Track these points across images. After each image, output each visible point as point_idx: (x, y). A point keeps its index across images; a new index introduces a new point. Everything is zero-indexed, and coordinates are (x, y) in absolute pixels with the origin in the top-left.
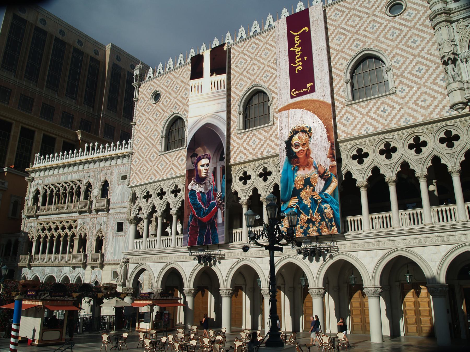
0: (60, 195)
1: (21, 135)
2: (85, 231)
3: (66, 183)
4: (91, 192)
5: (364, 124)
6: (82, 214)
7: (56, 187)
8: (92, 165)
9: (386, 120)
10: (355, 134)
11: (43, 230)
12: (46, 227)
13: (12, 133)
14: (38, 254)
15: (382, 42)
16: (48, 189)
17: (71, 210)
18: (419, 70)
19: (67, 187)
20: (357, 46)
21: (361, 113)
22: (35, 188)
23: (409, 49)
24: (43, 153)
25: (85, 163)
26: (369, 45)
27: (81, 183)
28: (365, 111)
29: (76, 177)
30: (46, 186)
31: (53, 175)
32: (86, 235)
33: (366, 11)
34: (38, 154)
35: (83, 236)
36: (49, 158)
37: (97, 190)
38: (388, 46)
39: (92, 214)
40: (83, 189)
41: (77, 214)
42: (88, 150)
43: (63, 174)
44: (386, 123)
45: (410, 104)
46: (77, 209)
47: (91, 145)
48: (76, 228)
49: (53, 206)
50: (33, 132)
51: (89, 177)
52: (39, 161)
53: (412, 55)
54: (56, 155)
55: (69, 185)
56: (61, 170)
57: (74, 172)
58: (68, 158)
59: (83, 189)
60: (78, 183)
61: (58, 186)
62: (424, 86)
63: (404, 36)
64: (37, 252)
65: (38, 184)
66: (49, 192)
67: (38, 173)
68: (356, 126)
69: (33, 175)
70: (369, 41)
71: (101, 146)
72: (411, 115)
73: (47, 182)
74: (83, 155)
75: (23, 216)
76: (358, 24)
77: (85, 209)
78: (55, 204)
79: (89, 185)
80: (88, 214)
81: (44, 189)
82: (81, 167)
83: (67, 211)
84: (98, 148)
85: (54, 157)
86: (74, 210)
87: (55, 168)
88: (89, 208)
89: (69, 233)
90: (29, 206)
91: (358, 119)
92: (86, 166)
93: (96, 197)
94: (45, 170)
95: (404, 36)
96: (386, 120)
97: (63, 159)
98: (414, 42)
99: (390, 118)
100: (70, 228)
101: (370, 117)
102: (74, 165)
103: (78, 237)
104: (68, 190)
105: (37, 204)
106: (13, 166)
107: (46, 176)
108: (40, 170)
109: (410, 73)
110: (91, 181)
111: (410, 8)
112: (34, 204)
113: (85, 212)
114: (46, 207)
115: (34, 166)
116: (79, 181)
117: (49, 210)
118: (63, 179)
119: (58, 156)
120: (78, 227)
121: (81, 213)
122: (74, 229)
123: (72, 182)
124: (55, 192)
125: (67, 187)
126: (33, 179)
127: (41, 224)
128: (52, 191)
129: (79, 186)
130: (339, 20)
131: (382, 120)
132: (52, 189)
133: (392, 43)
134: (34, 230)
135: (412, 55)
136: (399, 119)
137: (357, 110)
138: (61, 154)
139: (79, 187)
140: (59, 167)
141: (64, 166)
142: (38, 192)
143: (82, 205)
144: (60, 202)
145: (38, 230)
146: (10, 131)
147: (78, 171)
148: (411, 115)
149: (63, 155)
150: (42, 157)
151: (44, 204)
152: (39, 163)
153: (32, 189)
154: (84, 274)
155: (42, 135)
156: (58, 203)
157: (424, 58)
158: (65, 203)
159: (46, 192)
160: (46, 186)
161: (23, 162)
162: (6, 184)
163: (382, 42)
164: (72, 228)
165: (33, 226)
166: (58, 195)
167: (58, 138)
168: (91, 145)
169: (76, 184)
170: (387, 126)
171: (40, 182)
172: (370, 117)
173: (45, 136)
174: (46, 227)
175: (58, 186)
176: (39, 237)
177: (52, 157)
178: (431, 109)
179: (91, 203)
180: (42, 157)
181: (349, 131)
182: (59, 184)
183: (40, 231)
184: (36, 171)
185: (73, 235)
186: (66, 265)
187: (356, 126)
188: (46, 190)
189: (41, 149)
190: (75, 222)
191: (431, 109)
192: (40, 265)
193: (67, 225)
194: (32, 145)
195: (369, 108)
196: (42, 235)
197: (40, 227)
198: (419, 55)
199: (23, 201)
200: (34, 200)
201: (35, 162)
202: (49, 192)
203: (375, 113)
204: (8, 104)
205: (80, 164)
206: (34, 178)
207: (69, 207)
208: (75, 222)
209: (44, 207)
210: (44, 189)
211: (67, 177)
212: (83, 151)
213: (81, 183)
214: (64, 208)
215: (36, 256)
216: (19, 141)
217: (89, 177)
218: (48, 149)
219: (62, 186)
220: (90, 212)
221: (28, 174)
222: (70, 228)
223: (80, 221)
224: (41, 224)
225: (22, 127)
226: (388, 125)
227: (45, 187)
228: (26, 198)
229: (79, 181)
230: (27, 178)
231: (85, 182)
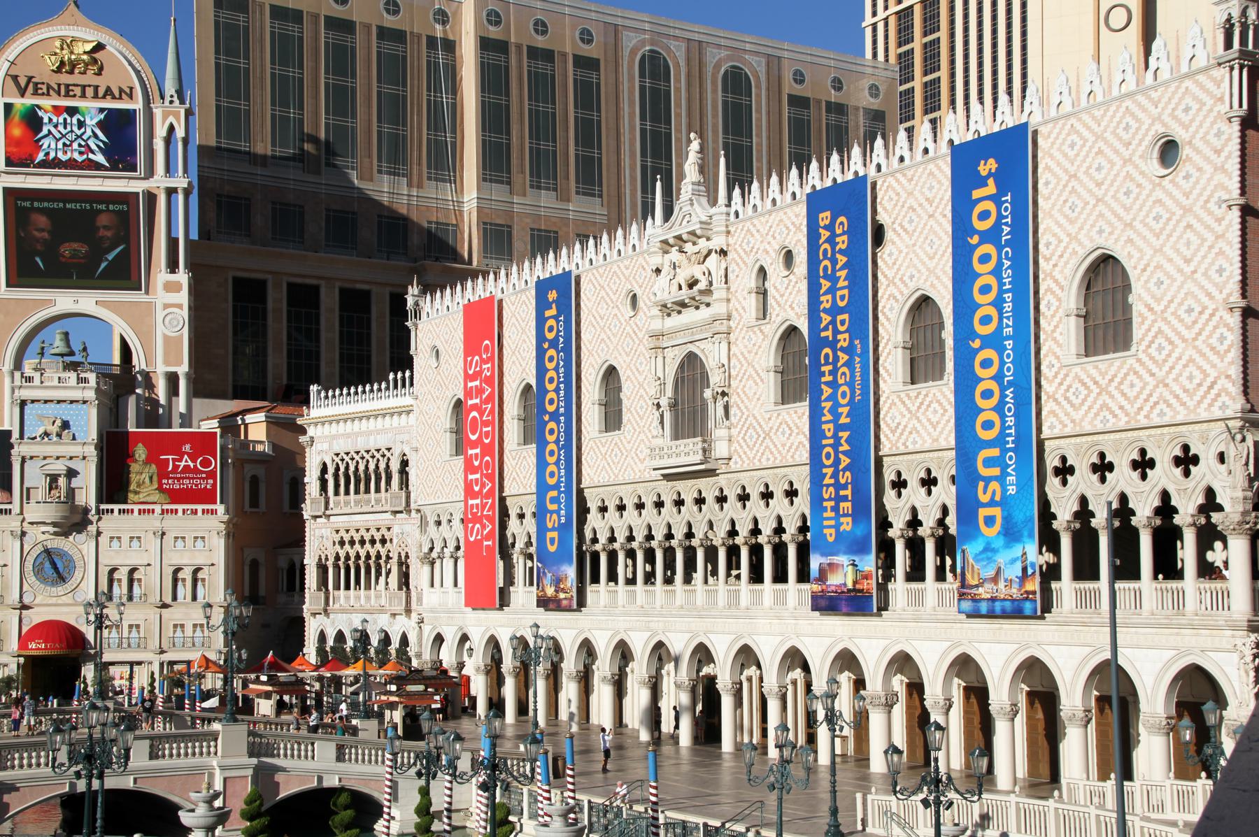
1: (289, 304)
11: (342, 543)
12: (347, 538)
13: (270, 305)
14: (339, 589)
30: (337, 455)
32: (407, 557)
40: (395, 466)
50: (316, 289)
64: (337, 587)
100: (383, 541)
103: (395, 559)
120: (395, 541)
127: (337, 531)
142: (324, 469)
146: (263, 300)
155: (337, 291)
167: (374, 289)
171: (325, 446)
173: (343, 292)
174: (347, 538)
176: (337, 558)
180: (323, 394)
183: (338, 547)
186: (382, 610)
192: (343, 611)
193: (378, 537)
194: (318, 323)
197: (337, 539)
208: (389, 529)
215: (336, 593)
216: (289, 321)
220: (409, 512)
222: (383, 541)
223: (396, 530)
224: (337, 531)
225: (290, 285)
229: (389, 449)
231: (397, 452)
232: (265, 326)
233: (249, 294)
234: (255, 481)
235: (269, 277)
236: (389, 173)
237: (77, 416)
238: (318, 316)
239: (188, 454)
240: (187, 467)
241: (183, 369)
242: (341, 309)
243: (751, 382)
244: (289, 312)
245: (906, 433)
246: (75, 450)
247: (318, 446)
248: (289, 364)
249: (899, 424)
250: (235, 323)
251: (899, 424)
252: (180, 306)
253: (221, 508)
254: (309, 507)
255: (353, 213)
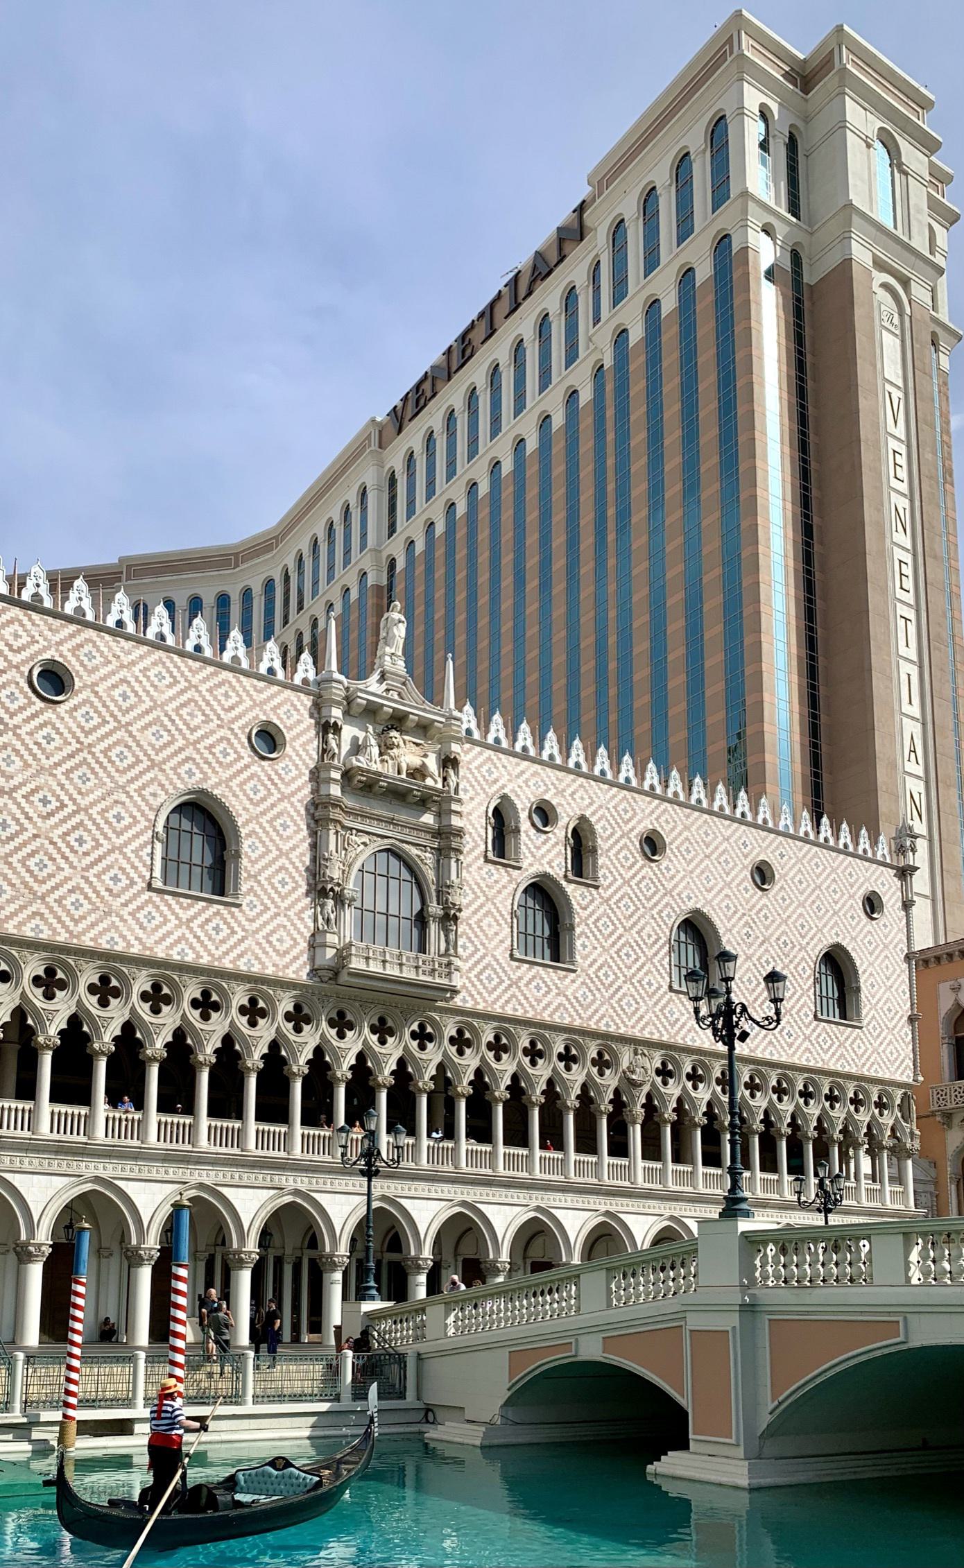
5: (178, 941)
9: (217, 948)
10: (160, 953)
15: (235, 795)
18: (283, 883)
20: (190, 773)
21: (177, 918)
23: (273, 834)
26: (213, 787)
28: (184, 915)
33: (220, 711)
38: (244, 809)
44: (218, 953)
45: (259, 936)
53: (278, 849)
62: (285, 915)
63: (273, 806)
68: (163, 939)
70: (214, 780)
72: (257, 958)
76: (199, 728)
91: (169, 926)
95: (273, 806)
96: (217, 948)
98: (285, 827)
99: (224, 948)
101: (191, 930)
109: (268, 879)
111: (290, 757)
130: (163, 692)
131: (211, 947)
133: (251, 807)
135: (278, 849)
136: (240, 956)
137: (169, 906)
148: (257, 958)
157: (293, 863)
163: (235, 795)
170: (217, 959)
172: (191, 930)
178: (288, 959)
181: (150, 942)
187: (163, 939)
191: (288, 959)
195: (192, 912)
198: (287, 855)
203: (201, 926)
226: (220, 959)
243: (489, 919)
245: (685, 1030)
249: (678, 1020)
251: (678, 1020)
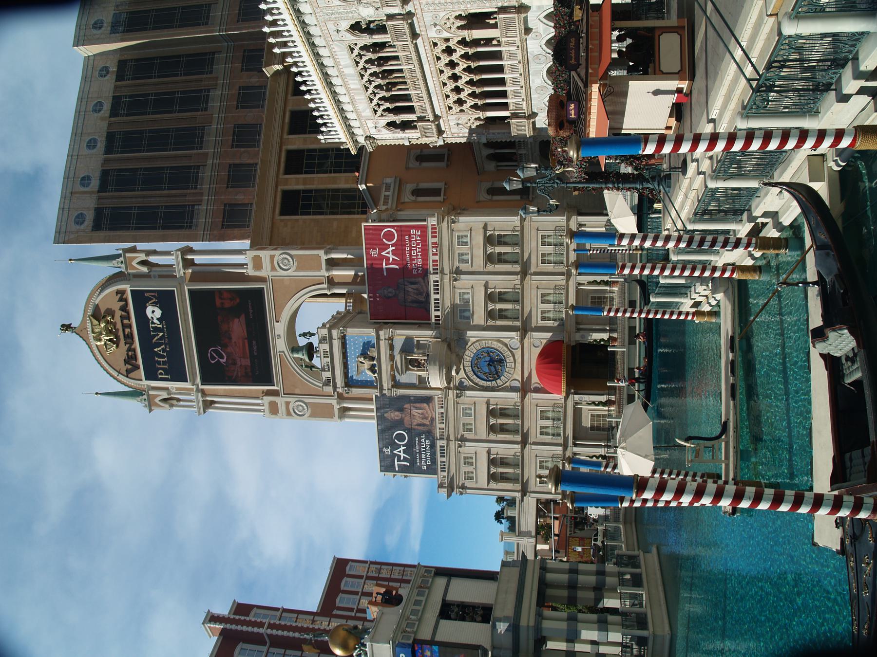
0: (388, 84)
2: (452, 20)
3: (362, 76)
4: (371, 22)
6: (418, 32)
7: (374, 94)
8: (312, 30)
11: (460, 102)
12: (454, 97)
13: (300, 187)
14: (506, 104)
16: (382, 108)
17: (414, 56)
19: (369, 71)
22: (385, 131)
24: (316, 129)
25: (313, 45)
27: (356, 44)
29: (345, 59)
31: (352, 102)
32: (459, 17)
34: (320, 137)
35: (462, 23)
36: (321, 117)
37: (361, 8)
39: (413, 11)
40: (367, 40)
41: (419, 41)
42: (285, 44)
43: (345, 85)
46: (409, 43)
47: (272, 40)
48: (447, 40)
49: (411, 92)
50: (289, 152)
51: (338, 31)
52: (333, 133)
54: (312, 105)
55: (365, 69)
56: (338, 90)
57: (337, 65)
58: (312, 81)
59: (367, 40)
60: (356, 52)
61: (370, 90)
65: (376, 127)
66: (387, 105)
67: (356, 131)
69: (361, 140)
71: (269, 18)
73: (368, 113)
74: (298, 52)
75: (441, 143)
77: (406, 26)
78: (407, 89)
79: (356, 27)
80: (415, 19)
81: (382, 115)
82: (322, 52)
83: (416, 63)
84: (274, 23)
85: (317, 109)
86: (412, 49)
87: (338, 102)
88: (403, 19)
89: (460, 51)
90: (419, 135)
92: (317, 41)
93: (377, 9)
94: (345, 119)
97: (316, 90)
100: (449, 51)
102: (322, 66)
103: (465, 34)
104: (374, 69)
105: (413, 121)
106: (357, 174)
107: (358, 115)
108: (349, 127)
110: (345, 25)
112: (415, 127)
113: (412, 26)
114: (415, 104)
115: (343, 140)
116: (352, 50)
117: (420, 99)
118: (356, 84)
119: (313, 100)
120: (446, 35)
121: (415, 35)
122: (450, 44)
123: (357, 63)
124: (383, 94)
125: (369, 71)
126: (368, 138)
127: (450, 108)
128: (383, 99)
129: (361, 48)
132: (380, 99)
134: (464, 118)
138: (307, 97)
139: (365, 48)
140: (334, 94)
141: (330, 85)
142: (391, 125)
143: (398, 35)
144: (401, 80)
145: (462, 111)
146: (297, 192)
147: (332, 56)
149: (309, 91)
150: (323, 129)
151: (411, 110)
152: (336, 133)
153: (388, 136)
154: (539, 7)
156: (405, 83)
158: (401, 71)
159: (387, 110)
160: (376, 111)
161: (341, 159)
162: (388, 180)
164: (448, 48)
165: (456, 122)
166: (390, 86)
167: (290, 107)
168: (272, 40)
169: (360, 56)
171: (370, 124)
173: (292, 131)
174: (454, 97)
175: (370, 90)
176: (475, 107)
177: (319, 111)
179: (390, 17)
180: (323, 129)
182: (367, 88)
183: (464, 107)
184: (352, 135)
185: (463, 42)
186: (523, 47)
188: (384, 110)
189: (310, 133)
190: (435, 44)
192: (529, 98)
193: (445, 59)
196: (471, 102)
197: (456, 108)
199: (412, 147)
200: (408, 129)
201: (337, 140)
202: (387, 105)
204: (252, 204)
205: (317, 56)
206: (366, 137)
207: (408, 59)
208: (435, 44)
209: (417, 109)
210: (382, 115)
211: (350, 75)
212: (290, 54)
213: (356, 44)
214: (412, 71)
215: (511, 107)
216: (313, 172)
217: (338, 31)
218: (306, 121)
219: (370, 82)
220: (410, 15)
221: (361, 149)
222: (449, 51)
223: (433, 34)
224: (450, 108)
227: (379, 113)
228: (407, 144)
229: (352, 50)
230: (370, 149)
231: (350, 38)
232: (316, 191)
233: (293, 203)
234: (417, 192)
235: (280, 188)
236: (207, 102)
237: (355, 344)
238: (309, 151)
239: (380, 252)
240: (394, 253)
241: (323, 255)
242: (305, 133)
244: (306, 173)
246: (384, 346)
247: (373, 132)
248: (345, 171)
250: (314, 214)
252: (272, 257)
253: (432, 221)
254: (432, 139)
255: (235, 127)
